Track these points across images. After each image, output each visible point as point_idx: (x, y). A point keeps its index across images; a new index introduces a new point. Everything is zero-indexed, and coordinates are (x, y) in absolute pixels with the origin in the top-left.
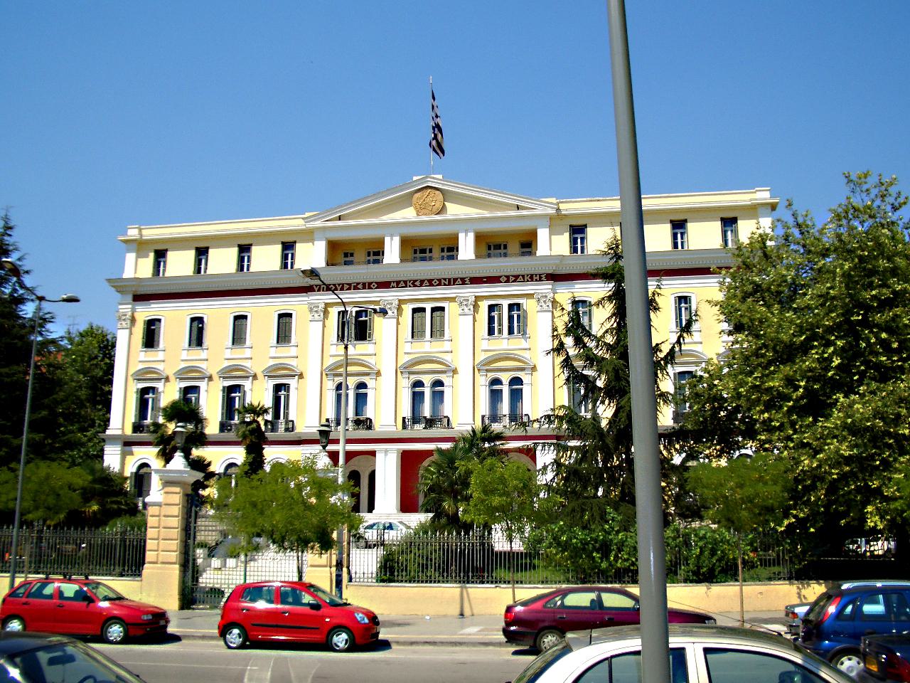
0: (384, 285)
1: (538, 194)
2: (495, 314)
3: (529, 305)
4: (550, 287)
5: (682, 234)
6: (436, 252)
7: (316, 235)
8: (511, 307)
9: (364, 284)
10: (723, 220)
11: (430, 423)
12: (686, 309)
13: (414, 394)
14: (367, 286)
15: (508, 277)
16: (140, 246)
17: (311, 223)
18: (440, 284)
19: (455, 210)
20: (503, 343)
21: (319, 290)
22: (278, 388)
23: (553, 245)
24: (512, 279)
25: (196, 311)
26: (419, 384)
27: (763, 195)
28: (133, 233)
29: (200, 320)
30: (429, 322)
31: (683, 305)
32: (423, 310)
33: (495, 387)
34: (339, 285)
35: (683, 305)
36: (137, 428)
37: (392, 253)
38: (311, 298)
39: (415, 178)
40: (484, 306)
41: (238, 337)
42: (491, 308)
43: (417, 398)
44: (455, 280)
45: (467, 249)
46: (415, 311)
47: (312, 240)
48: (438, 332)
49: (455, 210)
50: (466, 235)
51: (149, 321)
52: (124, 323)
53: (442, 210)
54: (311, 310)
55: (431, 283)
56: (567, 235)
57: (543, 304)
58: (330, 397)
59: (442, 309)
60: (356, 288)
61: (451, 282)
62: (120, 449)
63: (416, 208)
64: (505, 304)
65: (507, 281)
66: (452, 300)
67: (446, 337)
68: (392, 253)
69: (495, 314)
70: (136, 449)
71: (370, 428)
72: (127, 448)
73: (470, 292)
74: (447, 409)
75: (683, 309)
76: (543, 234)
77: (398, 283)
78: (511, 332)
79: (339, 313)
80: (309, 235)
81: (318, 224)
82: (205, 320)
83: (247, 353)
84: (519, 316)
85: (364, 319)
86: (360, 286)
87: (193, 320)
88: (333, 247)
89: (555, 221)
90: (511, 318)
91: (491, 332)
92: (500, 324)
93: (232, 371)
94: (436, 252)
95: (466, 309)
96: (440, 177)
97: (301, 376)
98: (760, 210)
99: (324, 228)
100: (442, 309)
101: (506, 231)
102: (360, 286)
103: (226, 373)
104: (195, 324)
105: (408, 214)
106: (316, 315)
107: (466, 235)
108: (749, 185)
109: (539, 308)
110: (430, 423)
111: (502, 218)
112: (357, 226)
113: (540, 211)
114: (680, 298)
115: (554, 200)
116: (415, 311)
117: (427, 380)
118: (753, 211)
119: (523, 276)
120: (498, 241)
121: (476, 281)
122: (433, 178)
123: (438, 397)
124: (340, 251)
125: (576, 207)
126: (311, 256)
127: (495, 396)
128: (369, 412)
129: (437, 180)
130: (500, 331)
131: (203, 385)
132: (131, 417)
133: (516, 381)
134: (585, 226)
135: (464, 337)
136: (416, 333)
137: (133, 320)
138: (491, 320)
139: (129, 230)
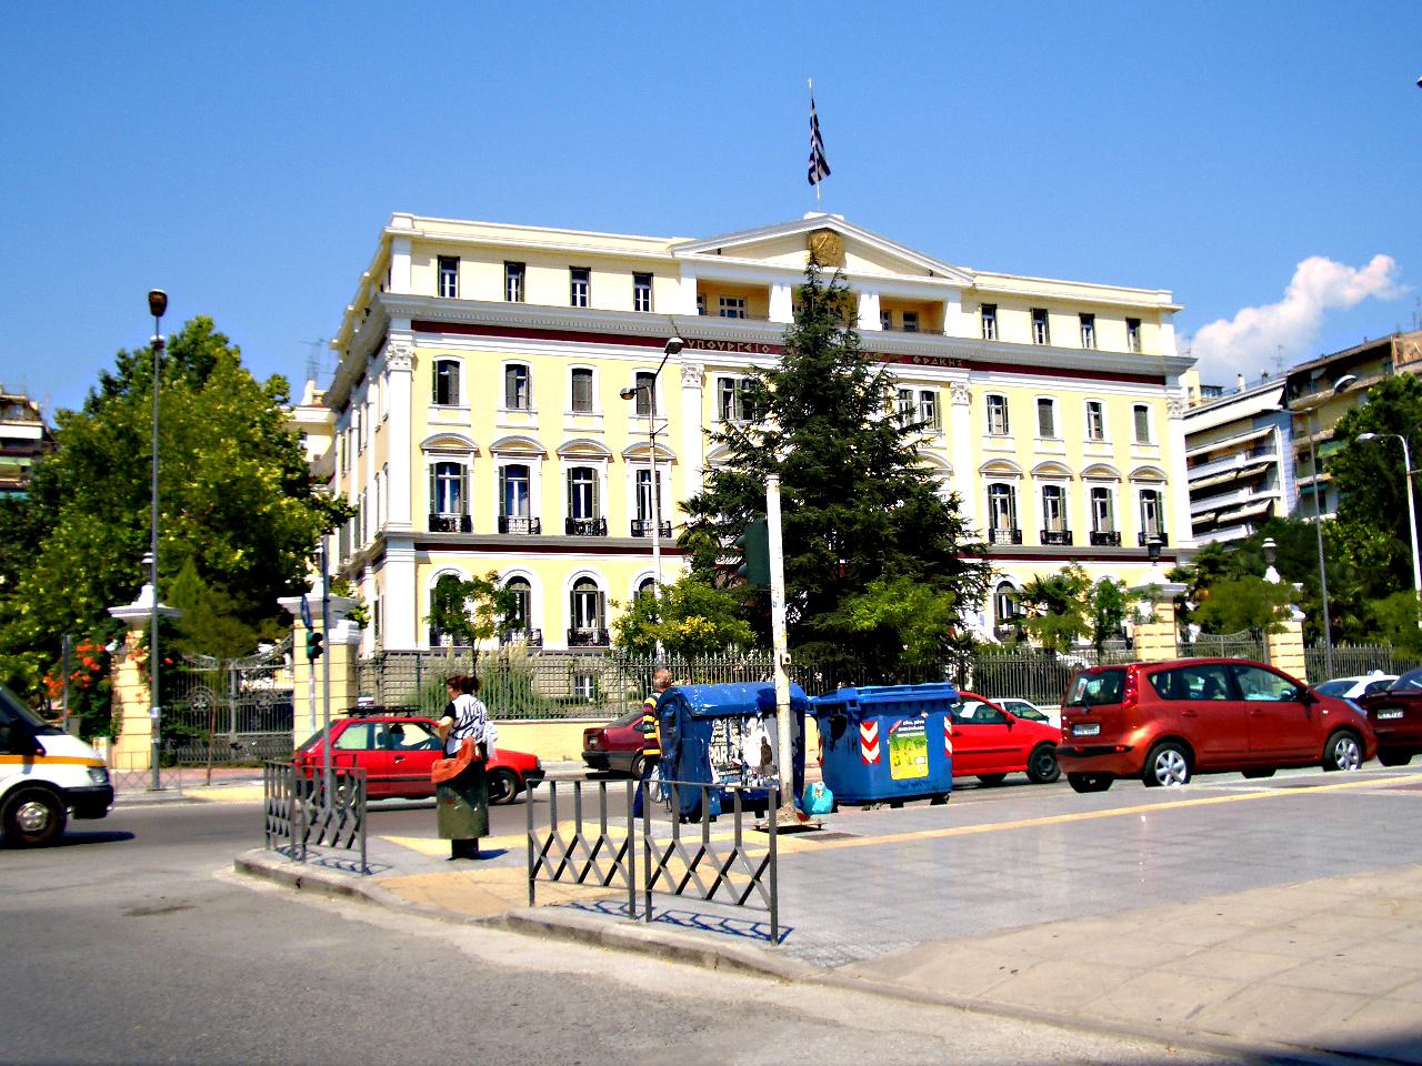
1: (953, 262)
3: (945, 396)
4: (967, 375)
7: (683, 268)
9: (753, 345)
10: (1128, 320)
15: (921, 358)
17: (683, 252)
21: (695, 347)
22: (644, 474)
23: (961, 324)
24: (926, 361)
25: (579, 361)
27: (1163, 299)
34: (721, 342)
36: (436, 523)
39: (811, 215)
47: (678, 276)
50: (870, 297)
52: (401, 363)
54: (684, 375)
56: (978, 315)
57: (959, 395)
60: (743, 349)
62: (413, 554)
64: (916, 390)
65: (921, 363)
70: (433, 555)
72: (422, 553)
79: (719, 379)
80: (674, 268)
81: (691, 255)
86: (748, 347)
88: (705, 292)
89: (968, 295)
93: (580, 447)
96: (841, 217)
98: (1163, 316)
99: (695, 263)
101: (903, 299)
102: (748, 347)
103: (568, 453)
107: (870, 297)
108: (1152, 285)
112: (740, 265)
113: (957, 281)
115: (969, 270)
118: (1156, 314)
119: (938, 359)
122: (836, 219)
125: (989, 283)
126: (675, 299)
132: (563, 511)
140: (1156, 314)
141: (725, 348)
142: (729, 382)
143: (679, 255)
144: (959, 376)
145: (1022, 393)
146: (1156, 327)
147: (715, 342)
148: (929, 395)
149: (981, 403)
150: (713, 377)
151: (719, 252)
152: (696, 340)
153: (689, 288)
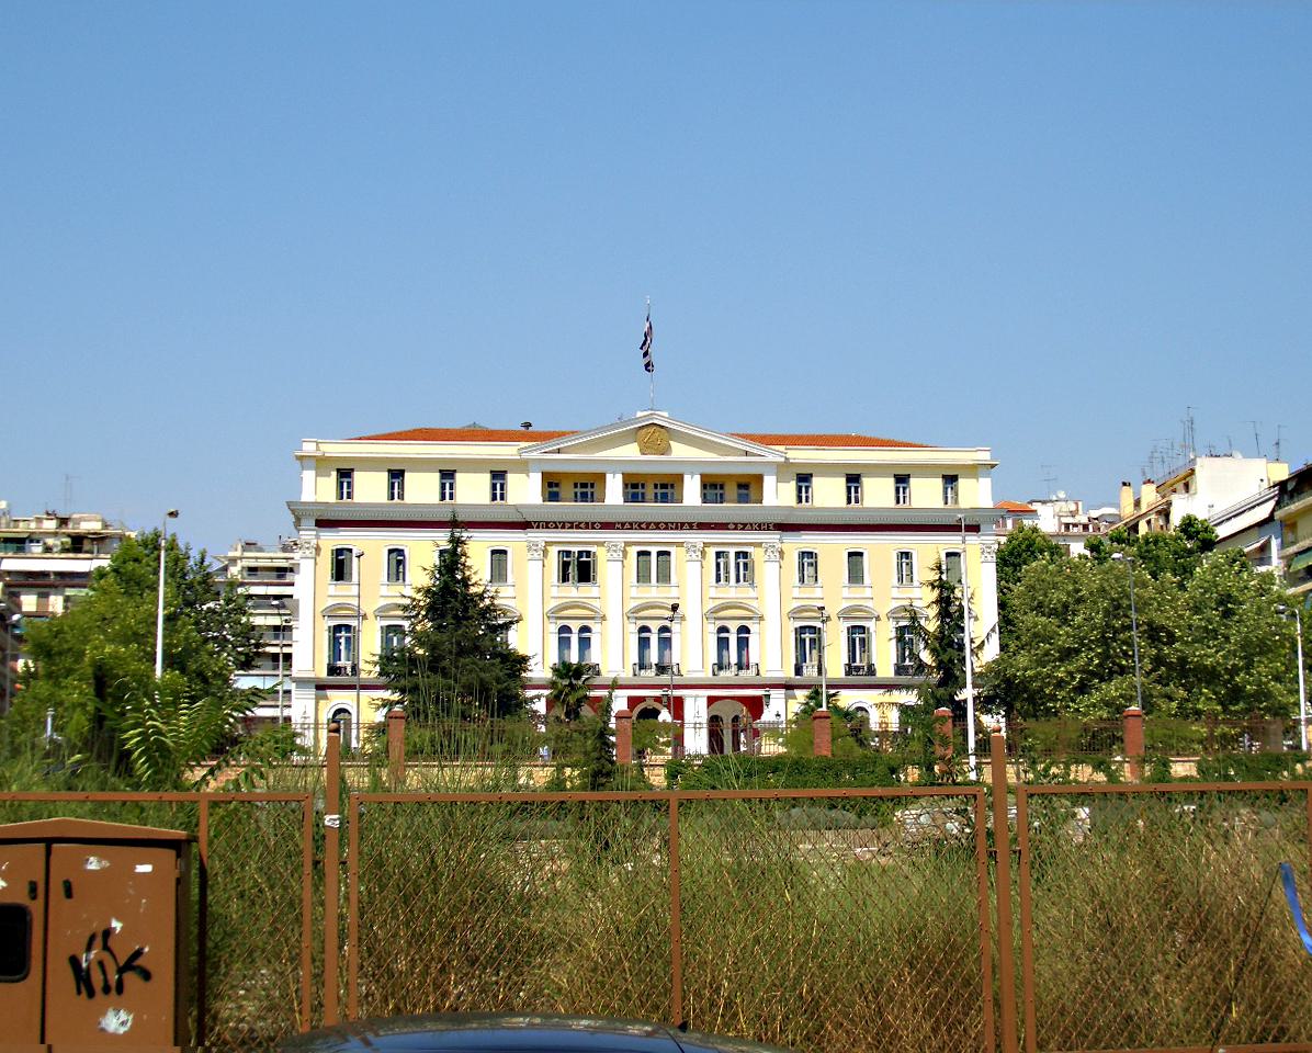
2: (721, 561)
5: (904, 489)
6: (650, 491)
8: (738, 554)
12: (907, 564)
14: (590, 526)
15: (736, 524)
16: (320, 464)
18: (666, 529)
19: (680, 451)
20: (732, 592)
21: (538, 527)
23: (778, 495)
27: (984, 456)
28: (309, 448)
29: (400, 552)
30: (653, 567)
31: (904, 560)
32: (648, 553)
33: (723, 635)
35: (904, 560)
37: (614, 491)
38: (529, 535)
39: (639, 414)
40: (711, 552)
41: (855, 573)
42: (718, 555)
43: (644, 644)
44: (683, 524)
45: (692, 491)
46: (640, 554)
48: (664, 576)
49: (680, 451)
51: (337, 550)
53: (666, 450)
55: (657, 526)
56: (793, 485)
58: (553, 641)
59: (668, 553)
60: (578, 527)
61: (679, 526)
63: (639, 446)
64: (732, 551)
66: (680, 544)
68: (614, 491)
69: (721, 561)
73: (698, 538)
74: (676, 655)
75: (904, 565)
76: (769, 482)
77: (623, 524)
78: (738, 581)
80: (523, 466)
81: (535, 455)
82: (406, 553)
83: (867, 593)
84: (746, 565)
85: (584, 559)
86: (582, 525)
87: (390, 551)
89: (782, 469)
90: (738, 565)
91: (718, 580)
92: (727, 572)
94: (650, 491)
95: (694, 555)
96: (666, 414)
98: (980, 469)
100: (668, 553)
104: (394, 555)
105: (630, 452)
106: (536, 554)
109: (766, 558)
111: (731, 461)
112: (572, 459)
113: (770, 458)
114: (902, 553)
116: (640, 554)
118: (974, 470)
120: (719, 481)
121: (703, 526)
123: (665, 643)
124: (552, 486)
126: (525, 491)
127: (723, 644)
129: (662, 417)
130: (727, 579)
133: (744, 629)
134: (811, 475)
136: (642, 577)
137: (318, 549)
138: (718, 565)
139: (304, 444)
140: (974, 470)
141: (563, 527)
142: (568, 553)
143: (525, 456)
146: (975, 480)
147: (555, 523)
148: (745, 555)
149: (792, 560)
150: (553, 551)
151: (559, 451)
152: (539, 522)
153: (536, 479)
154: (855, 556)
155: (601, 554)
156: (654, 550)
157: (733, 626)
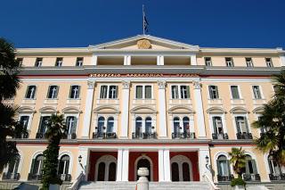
0: (123, 74)
8: (182, 87)
11: (146, 135)
13: (137, 123)
26: (140, 119)
30: (144, 92)
41: (235, 95)
42: (173, 87)
48: (148, 95)
64: (179, 85)
67: (153, 97)
71: (115, 137)
73: (164, 79)
91: (173, 97)
92: (177, 93)
97: (82, 112)
110: (146, 135)
117: (144, 117)
127: (176, 125)
128: (115, 130)
131: (31, 116)
133: (186, 119)
135: (161, 99)
136: (138, 96)
140: (277, 55)
144: (197, 79)
145: (224, 85)
148: (185, 87)
154: (234, 88)
155: (120, 86)
156: (144, 85)
157: (181, 117)
